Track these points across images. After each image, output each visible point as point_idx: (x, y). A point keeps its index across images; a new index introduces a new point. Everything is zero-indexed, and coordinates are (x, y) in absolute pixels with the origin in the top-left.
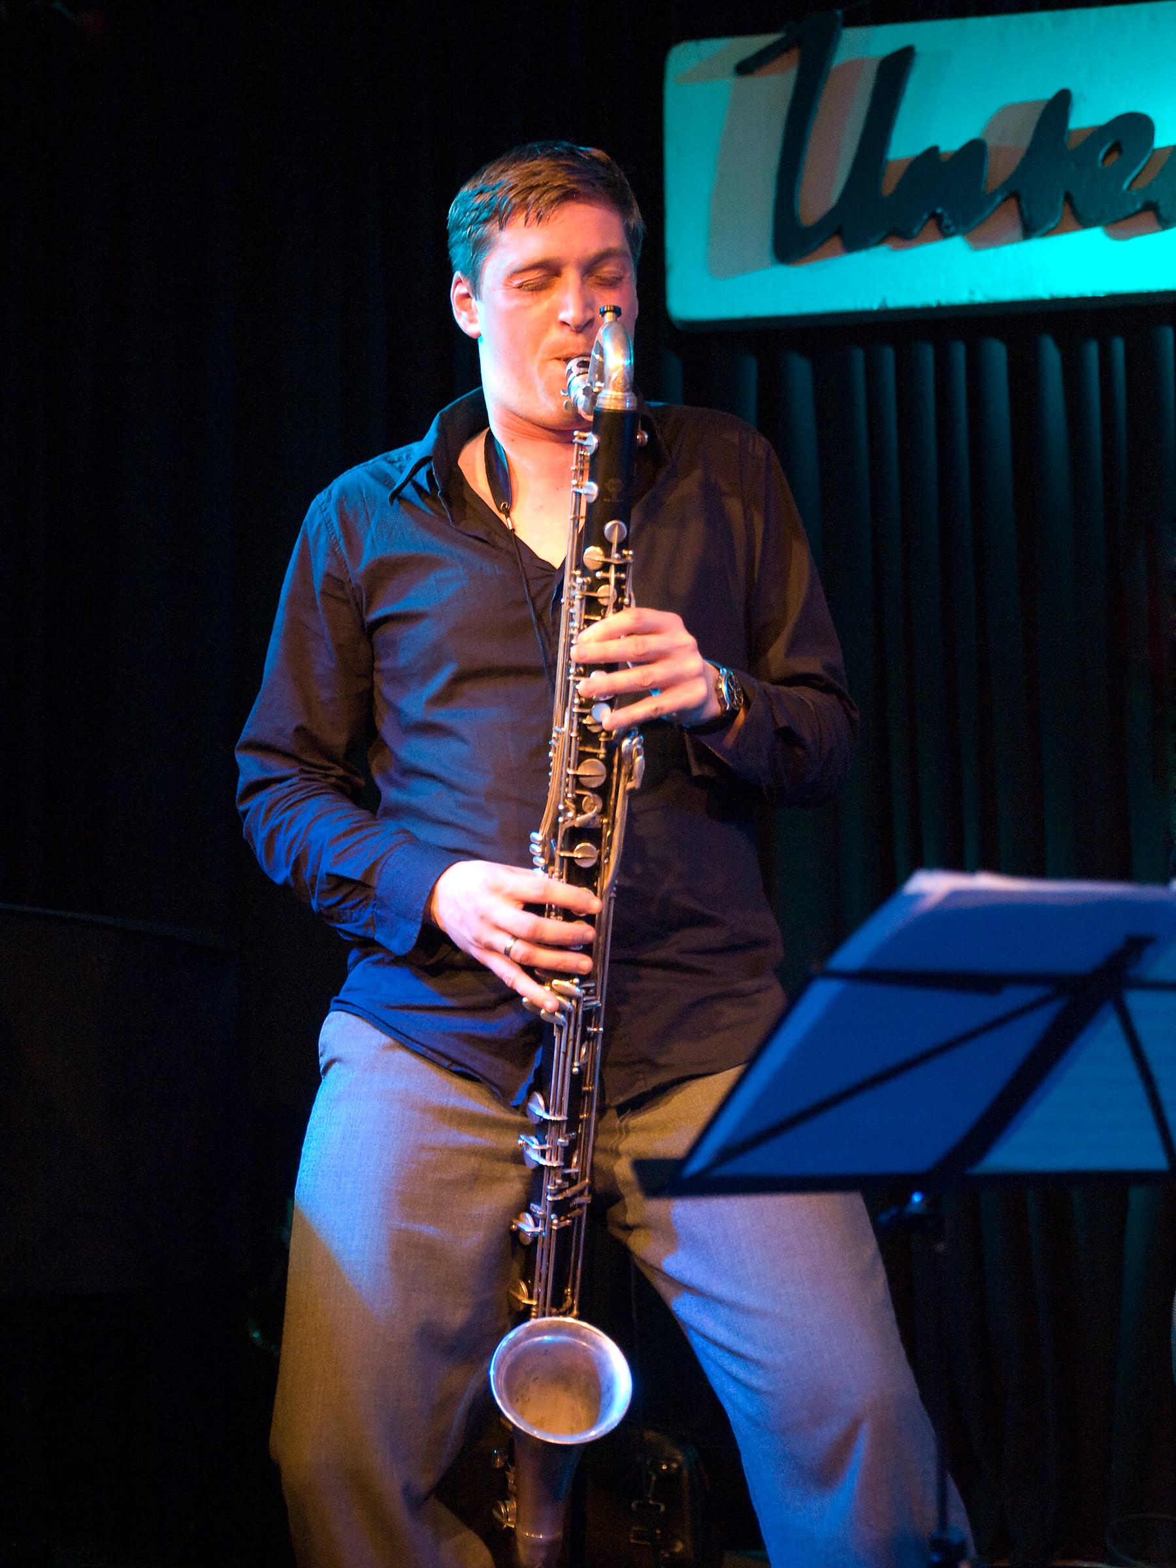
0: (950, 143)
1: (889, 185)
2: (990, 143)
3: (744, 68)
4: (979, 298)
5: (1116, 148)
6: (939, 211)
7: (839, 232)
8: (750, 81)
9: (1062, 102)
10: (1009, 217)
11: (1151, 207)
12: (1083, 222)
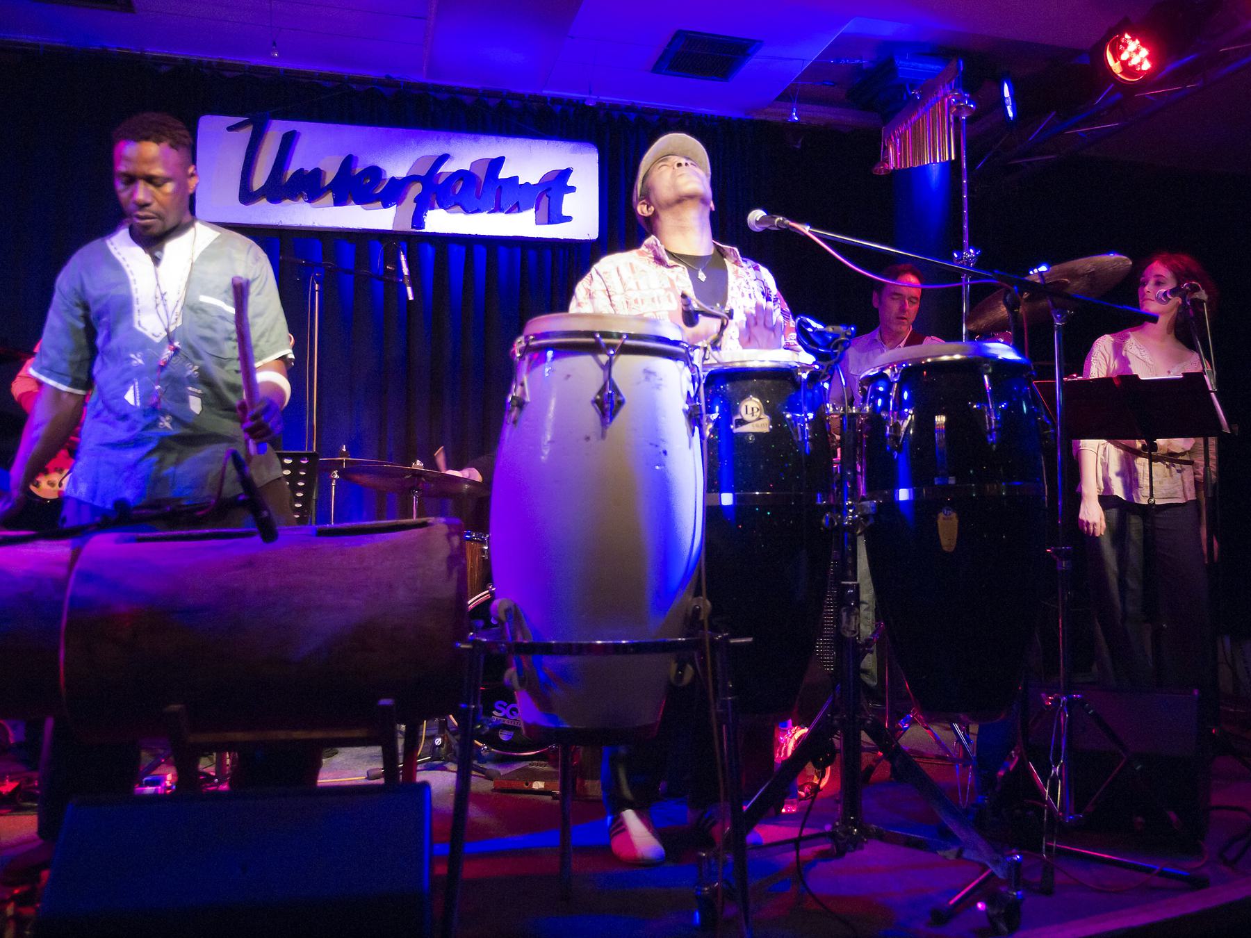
0: (309, 169)
3: (230, 129)
4: (316, 225)
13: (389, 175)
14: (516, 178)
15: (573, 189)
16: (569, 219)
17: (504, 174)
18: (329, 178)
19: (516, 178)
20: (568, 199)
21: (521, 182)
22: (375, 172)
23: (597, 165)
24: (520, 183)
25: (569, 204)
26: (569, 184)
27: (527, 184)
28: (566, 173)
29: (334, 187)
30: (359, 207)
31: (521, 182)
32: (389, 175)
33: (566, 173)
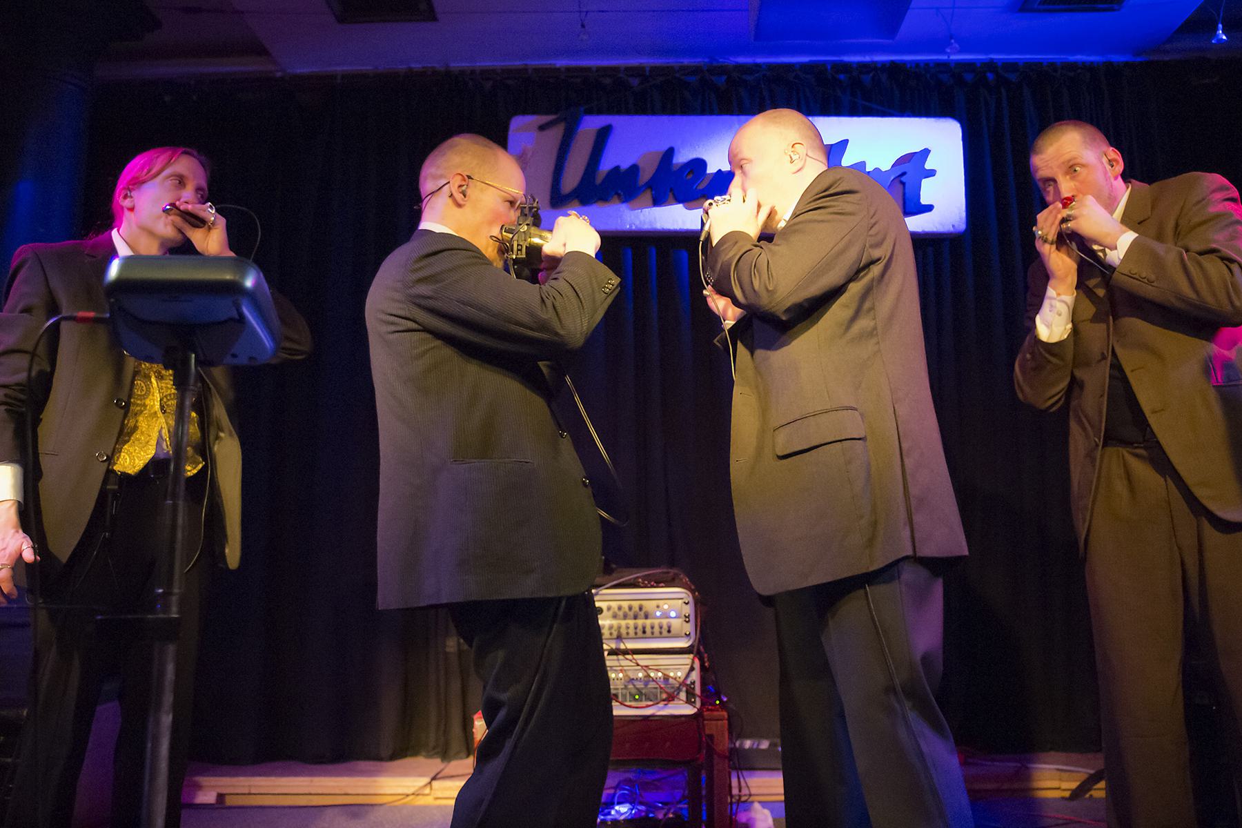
0: (625, 165)
1: (600, 177)
2: (641, 165)
3: (542, 128)
5: (692, 171)
7: (577, 197)
8: (545, 133)
9: (670, 152)
10: (647, 196)
12: (679, 201)
13: (711, 169)
14: (862, 165)
15: (932, 173)
16: (929, 208)
17: (848, 160)
18: (645, 176)
19: (862, 165)
20: (925, 183)
21: (869, 168)
22: (700, 164)
23: (961, 143)
24: (867, 170)
25: (928, 191)
26: (928, 166)
27: (877, 170)
28: (926, 152)
29: (650, 185)
30: (679, 208)
31: (869, 168)
32: (711, 169)
33: (926, 152)
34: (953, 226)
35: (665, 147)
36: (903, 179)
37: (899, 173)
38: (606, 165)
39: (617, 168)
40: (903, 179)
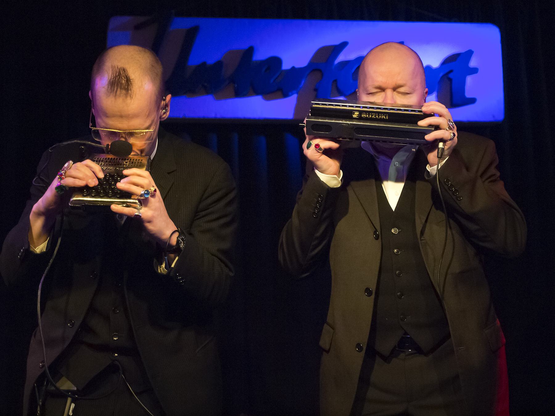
0: (211, 61)
3: (137, 27)
4: (218, 116)
6: (206, 84)
9: (250, 51)
11: (279, 89)
12: (257, 92)
13: (286, 66)
15: (474, 71)
16: (472, 101)
22: (276, 62)
28: (469, 53)
32: (286, 66)
33: (469, 53)
34: (494, 117)
35: (245, 46)
36: (451, 76)
37: (446, 71)
38: (194, 61)
39: (204, 64)
40: (451, 76)
